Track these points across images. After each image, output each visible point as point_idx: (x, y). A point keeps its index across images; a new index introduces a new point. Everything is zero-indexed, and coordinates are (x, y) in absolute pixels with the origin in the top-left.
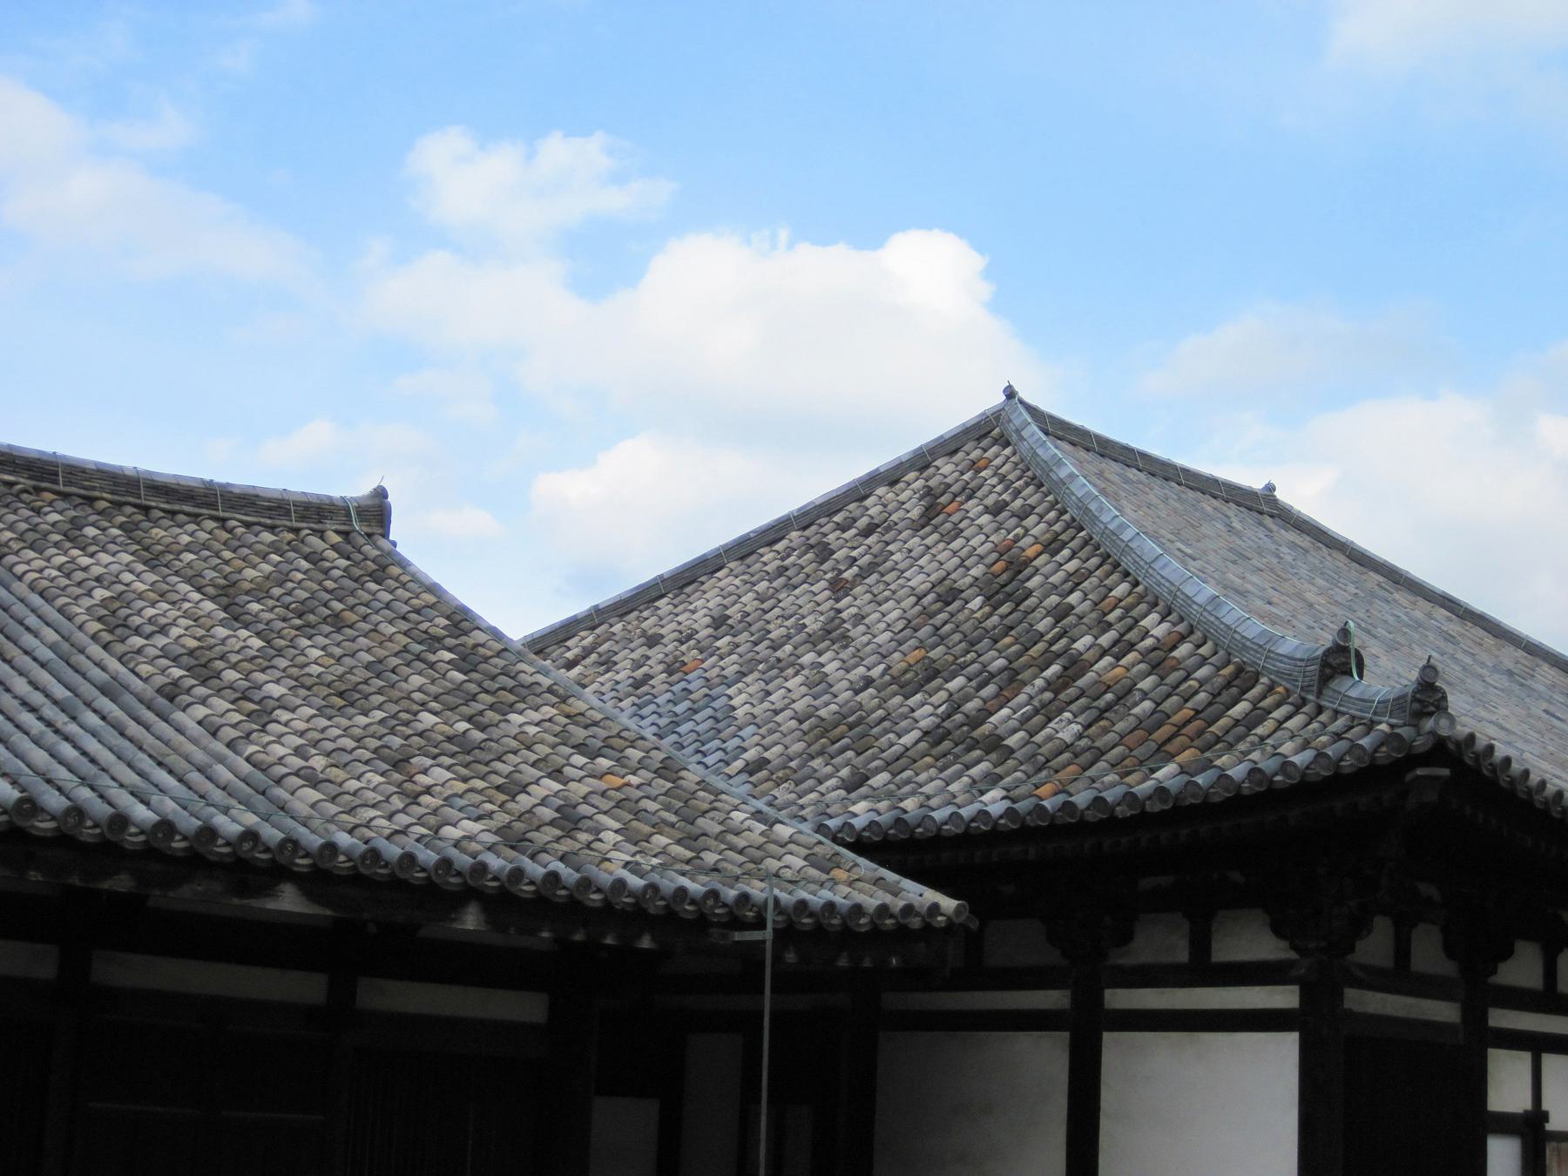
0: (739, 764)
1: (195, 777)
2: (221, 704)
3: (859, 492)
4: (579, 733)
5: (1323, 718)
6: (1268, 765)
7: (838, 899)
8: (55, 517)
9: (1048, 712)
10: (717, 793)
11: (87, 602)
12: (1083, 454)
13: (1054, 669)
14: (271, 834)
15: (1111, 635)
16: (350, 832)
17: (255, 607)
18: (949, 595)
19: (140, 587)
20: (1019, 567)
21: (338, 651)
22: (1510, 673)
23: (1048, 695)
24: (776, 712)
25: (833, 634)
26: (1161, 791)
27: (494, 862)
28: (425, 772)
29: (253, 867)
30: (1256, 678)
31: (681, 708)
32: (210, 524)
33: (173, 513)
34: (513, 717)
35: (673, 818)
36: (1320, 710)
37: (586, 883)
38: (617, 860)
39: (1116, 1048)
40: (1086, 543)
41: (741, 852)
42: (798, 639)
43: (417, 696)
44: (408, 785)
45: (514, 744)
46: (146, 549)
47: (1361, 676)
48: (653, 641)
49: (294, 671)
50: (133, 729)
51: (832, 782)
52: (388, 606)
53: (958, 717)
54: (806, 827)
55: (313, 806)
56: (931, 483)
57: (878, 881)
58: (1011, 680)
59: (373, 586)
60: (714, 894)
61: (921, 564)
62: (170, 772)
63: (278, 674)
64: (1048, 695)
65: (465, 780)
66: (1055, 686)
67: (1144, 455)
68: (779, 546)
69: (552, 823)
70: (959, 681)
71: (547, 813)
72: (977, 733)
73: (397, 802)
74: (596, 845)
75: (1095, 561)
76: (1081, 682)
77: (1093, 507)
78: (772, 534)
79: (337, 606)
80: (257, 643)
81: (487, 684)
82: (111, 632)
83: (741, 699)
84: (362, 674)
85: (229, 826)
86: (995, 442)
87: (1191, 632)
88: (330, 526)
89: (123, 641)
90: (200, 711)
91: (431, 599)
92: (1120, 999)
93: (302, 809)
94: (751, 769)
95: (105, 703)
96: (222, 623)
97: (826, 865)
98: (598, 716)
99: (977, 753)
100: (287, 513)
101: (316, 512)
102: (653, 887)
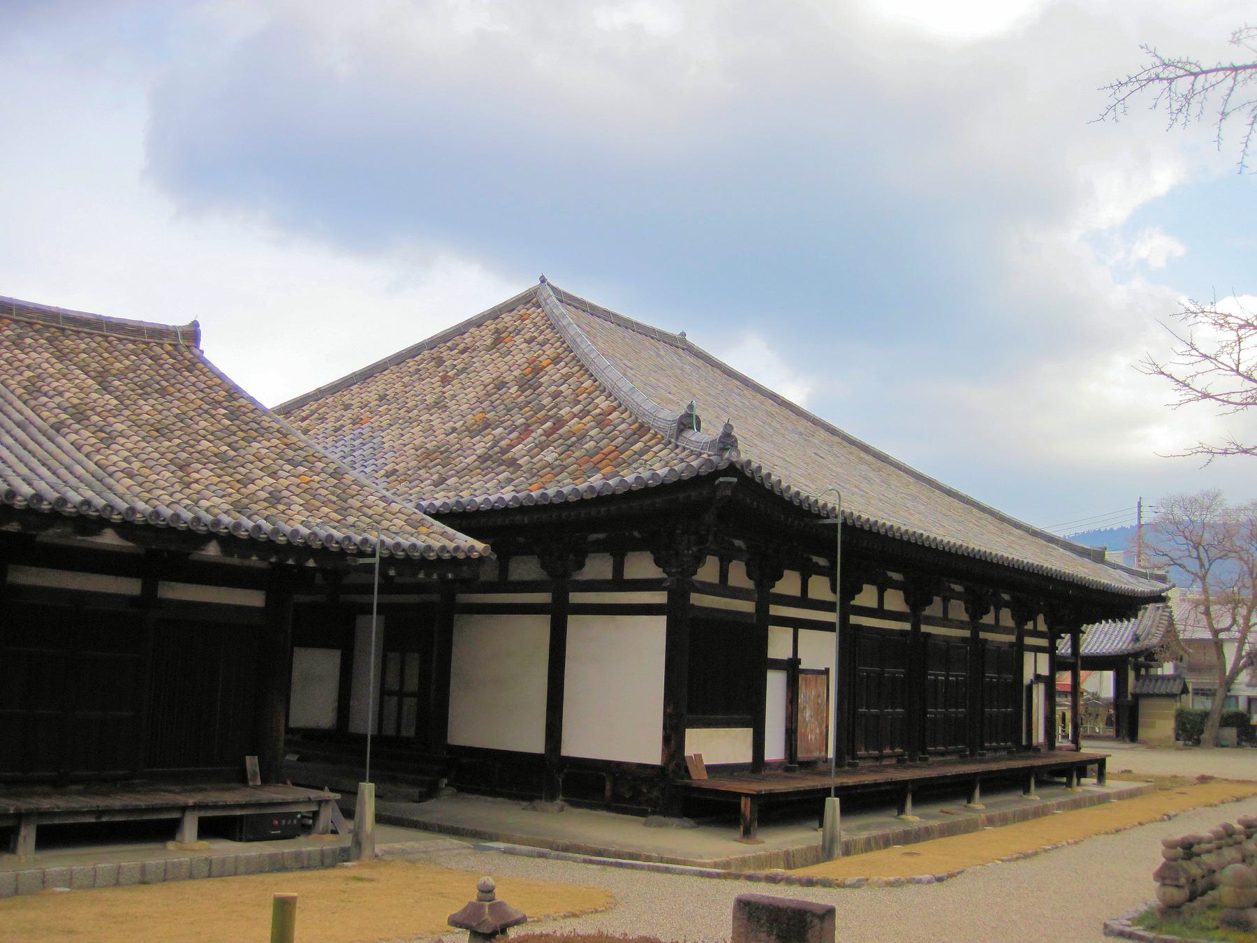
0: (383, 472)
1: (62, 471)
2: (86, 433)
3: (461, 330)
4: (290, 453)
5: (677, 451)
6: (645, 474)
7: (419, 543)
8: (8, 333)
9: (542, 447)
10: (362, 487)
11: (19, 378)
12: (581, 313)
13: (549, 424)
14: (99, 502)
15: (579, 407)
16: (146, 502)
17: (117, 383)
18: (501, 385)
19: (52, 371)
20: (537, 370)
21: (160, 407)
22: (801, 434)
23: (544, 438)
25: (440, 405)
26: (591, 488)
27: (226, 519)
28: (198, 472)
29: (88, 521)
30: (649, 429)
31: (357, 443)
32: (99, 339)
33: (79, 332)
34: (254, 444)
35: (334, 499)
36: (677, 446)
37: (276, 531)
38: (299, 521)
39: (573, 622)
40: (573, 358)
41: (370, 517)
42: (421, 407)
43: (202, 432)
44: (186, 479)
45: (252, 458)
46: (60, 351)
47: (699, 430)
48: (347, 407)
49: (134, 417)
50: (32, 445)
51: (428, 482)
52: (194, 385)
53: (497, 449)
54: (411, 506)
55: (128, 488)
57: (443, 534)
58: (526, 430)
59: (187, 374)
60: (349, 538)
61: (488, 368)
62: (49, 469)
63: (123, 418)
65: (219, 477)
66: (548, 434)
67: (615, 315)
69: (265, 500)
70: (500, 430)
71: (263, 495)
72: (504, 457)
73: (178, 487)
74: (288, 512)
75: (576, 368)
76: (561, 431)
79: (164, 383)
80: (115, 402)
81: (244, 427)
82: (30, 394)
83: (389, 438)
84: (173, 419)
85: (74, 497)
87: (620, 405)
88: (166, 341)
89: (36, 399)
90: (73, 437)
91: (219, 381)
92: (576, 598)
93: (120, 488)
94: (388, 475)
95: (19, 432)
96: (96, 391)
97: (416, 525)
98: (302, 445)
100: (143, 334)
101: (159, 333)
102: (314, 534)
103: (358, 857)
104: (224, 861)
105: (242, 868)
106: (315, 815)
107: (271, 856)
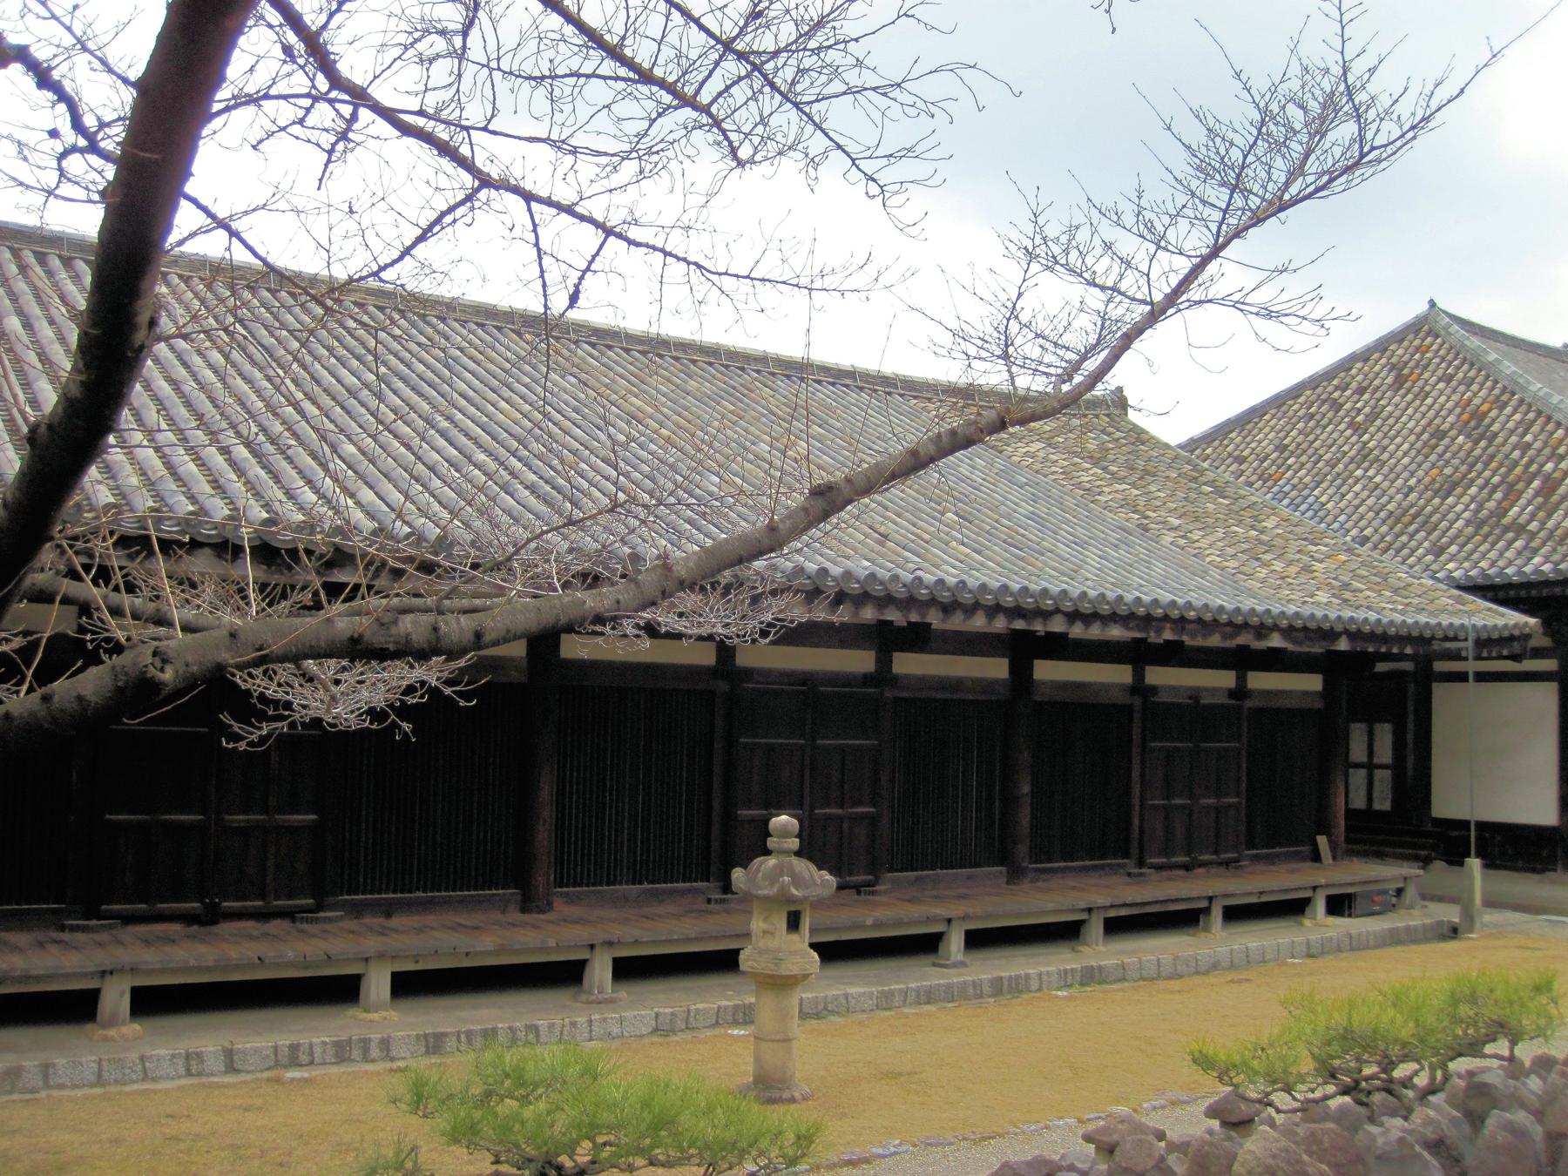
3: (1346, 365)
13: (1536, 484)
20: (1478, 416)
24: (1357, 507)
25: (1364, 456)
40: (1521, 401)
56: (1393, 360)
64: (1540, 500)
68: (1301, 400)
72: (1505, 521)
77: (1521, 380)
78: (1295, 392)
86: (1428, 334)
99: (1511, 535)
103: (1471, 930)
105: (1372, 943)
106: (1399, 892)
107: (1391, 931)
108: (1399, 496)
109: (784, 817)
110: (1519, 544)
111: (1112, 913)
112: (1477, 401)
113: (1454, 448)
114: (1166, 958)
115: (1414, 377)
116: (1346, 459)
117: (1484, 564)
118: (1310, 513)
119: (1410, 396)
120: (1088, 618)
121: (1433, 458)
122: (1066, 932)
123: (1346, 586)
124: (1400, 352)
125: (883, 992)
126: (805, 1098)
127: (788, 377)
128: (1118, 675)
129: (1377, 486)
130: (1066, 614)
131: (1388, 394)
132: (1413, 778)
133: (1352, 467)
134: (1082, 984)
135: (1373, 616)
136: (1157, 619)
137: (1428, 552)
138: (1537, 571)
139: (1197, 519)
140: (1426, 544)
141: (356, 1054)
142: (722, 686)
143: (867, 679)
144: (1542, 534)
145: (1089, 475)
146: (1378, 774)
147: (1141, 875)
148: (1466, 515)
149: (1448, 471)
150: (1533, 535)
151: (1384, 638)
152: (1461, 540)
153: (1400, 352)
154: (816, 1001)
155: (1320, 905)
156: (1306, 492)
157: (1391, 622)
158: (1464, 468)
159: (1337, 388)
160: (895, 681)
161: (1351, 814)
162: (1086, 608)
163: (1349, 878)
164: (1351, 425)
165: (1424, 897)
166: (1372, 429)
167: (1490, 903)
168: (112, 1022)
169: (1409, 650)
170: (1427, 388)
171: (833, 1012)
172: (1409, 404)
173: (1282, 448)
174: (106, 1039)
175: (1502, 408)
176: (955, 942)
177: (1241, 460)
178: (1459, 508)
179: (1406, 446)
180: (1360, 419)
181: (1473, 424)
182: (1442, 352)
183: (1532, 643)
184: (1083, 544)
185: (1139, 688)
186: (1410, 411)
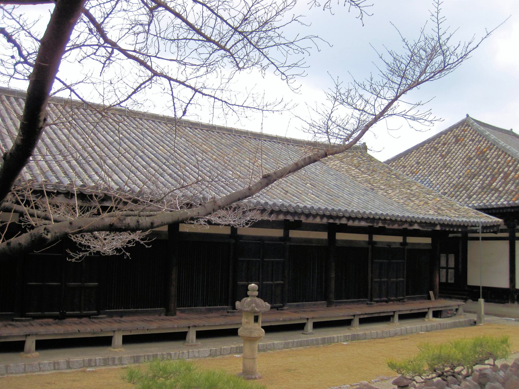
3: (439, 136)
13: (502, 175)
20: (483, 153)
24: (443, 183)
25: (445, 166)
40: (497, 148)
56: (455, 134)
64: (503, 180)
68: (424, 147)
72: (492, 187)
77: (497, 141)
86: (466, 126)
99: (493, 192)
104: (444, 324)
106: (457, 310)
107: (454, 322)
108: (457, 179)
109: (253, 285)
110: (496, 195)
111: (362, 317)
112: (482, 148)
113: (475, 163)
114: (379, 331)
115: (461, 140)
116: (439, 167)
117: (484, 201)
118: (427, 184)
119: (460, 146)
120: (354, 219)
121: (468, 166)
122: (346, 323)
123: (439, 209)
124: (457, 131)
125: (285, 343)
126: (260, 378)
127: (255, 139)
128: (363, 238)
129: (449, 176)
130: (346, 218)
131: (453, 145)
132: (461, 271)
133: (441, 169)
134: (352, 340)
135: (448, 219)
136: (377, 219)
137: (466, 198)
138: (502, 204)
139: (390, 186)
140: (466, 195)
141: (110, 363)
142: (233, 241)
143: (280, 239)
144: (504, 192)
145: (354, 171)
146: (450, 271)
147: (371, 304)
148: (479, 185)
149: (473, 171)
150: (501, 192)
151: (452, 226)
152: (477, 193)
153: (457, 131)
154: (263, 345)
155: (430, 314)
156: (426, 177)
157: (454, 221)
158: (478, 170)
159: (436, 143)
160: (290, 239)
161: (441, 284)
162: (353, 216)
163: (440, 305)
164: (441, 155)
165: (465, 311)
166: (448, 157)
167: (487, 314)
168: (29, 352)
169: (460, 230)
170: (466, 143)
171: (269, 349)
172: (460, 149)
173: (418, 163)
174: (27, 357)
175: (490, 150)
176: (309, 326)
177: (404, 167)
178: (477, 183)
179: (459, 162)
180: (443, 154)
181: (481, 155)
182: (471, 132)
183: (501, 228)
184: (352, 194)
185: (371, 242)
186: (460, 151)
